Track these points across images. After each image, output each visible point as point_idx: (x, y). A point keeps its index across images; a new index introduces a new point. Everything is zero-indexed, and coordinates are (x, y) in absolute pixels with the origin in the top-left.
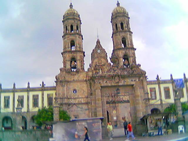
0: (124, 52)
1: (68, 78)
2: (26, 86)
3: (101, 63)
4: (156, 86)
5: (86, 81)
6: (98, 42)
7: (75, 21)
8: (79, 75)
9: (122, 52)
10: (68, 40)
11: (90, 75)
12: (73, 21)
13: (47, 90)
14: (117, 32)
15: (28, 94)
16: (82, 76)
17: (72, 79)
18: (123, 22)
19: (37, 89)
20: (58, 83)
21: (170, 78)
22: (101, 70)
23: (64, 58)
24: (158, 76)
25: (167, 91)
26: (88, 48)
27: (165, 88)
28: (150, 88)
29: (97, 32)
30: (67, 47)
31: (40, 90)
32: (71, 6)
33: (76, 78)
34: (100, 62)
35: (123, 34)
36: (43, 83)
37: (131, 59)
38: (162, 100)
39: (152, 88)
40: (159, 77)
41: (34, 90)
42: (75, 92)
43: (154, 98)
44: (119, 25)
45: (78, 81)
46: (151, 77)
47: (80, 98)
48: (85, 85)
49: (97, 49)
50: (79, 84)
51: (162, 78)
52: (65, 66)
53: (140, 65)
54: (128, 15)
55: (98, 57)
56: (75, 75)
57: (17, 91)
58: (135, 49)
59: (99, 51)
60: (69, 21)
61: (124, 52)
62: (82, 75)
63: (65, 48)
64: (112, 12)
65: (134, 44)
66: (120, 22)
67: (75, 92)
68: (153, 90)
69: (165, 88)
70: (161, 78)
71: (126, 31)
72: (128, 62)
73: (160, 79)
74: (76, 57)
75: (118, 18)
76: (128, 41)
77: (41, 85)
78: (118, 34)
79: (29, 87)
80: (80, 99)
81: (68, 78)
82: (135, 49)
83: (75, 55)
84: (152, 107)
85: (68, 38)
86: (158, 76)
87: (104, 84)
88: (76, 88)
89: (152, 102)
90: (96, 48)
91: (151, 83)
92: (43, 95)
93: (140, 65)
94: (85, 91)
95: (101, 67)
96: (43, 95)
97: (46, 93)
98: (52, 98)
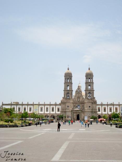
0: (89, 91)
4: (101, 107)
5: (73, 103)
13: (57, 105)
26: (75, 88)
29: (79, 82)
35: (89, 84)
46: (98, 102)
52: (65, 96)
54: (93, 75)
58: (94, 90)
60: (67, 77)
64: (86, 73)
66: (89, 76)
69: (104, 107)
82: (94, 90)
89: (99, 113)
91: (99, 105)
93: (95, 98)
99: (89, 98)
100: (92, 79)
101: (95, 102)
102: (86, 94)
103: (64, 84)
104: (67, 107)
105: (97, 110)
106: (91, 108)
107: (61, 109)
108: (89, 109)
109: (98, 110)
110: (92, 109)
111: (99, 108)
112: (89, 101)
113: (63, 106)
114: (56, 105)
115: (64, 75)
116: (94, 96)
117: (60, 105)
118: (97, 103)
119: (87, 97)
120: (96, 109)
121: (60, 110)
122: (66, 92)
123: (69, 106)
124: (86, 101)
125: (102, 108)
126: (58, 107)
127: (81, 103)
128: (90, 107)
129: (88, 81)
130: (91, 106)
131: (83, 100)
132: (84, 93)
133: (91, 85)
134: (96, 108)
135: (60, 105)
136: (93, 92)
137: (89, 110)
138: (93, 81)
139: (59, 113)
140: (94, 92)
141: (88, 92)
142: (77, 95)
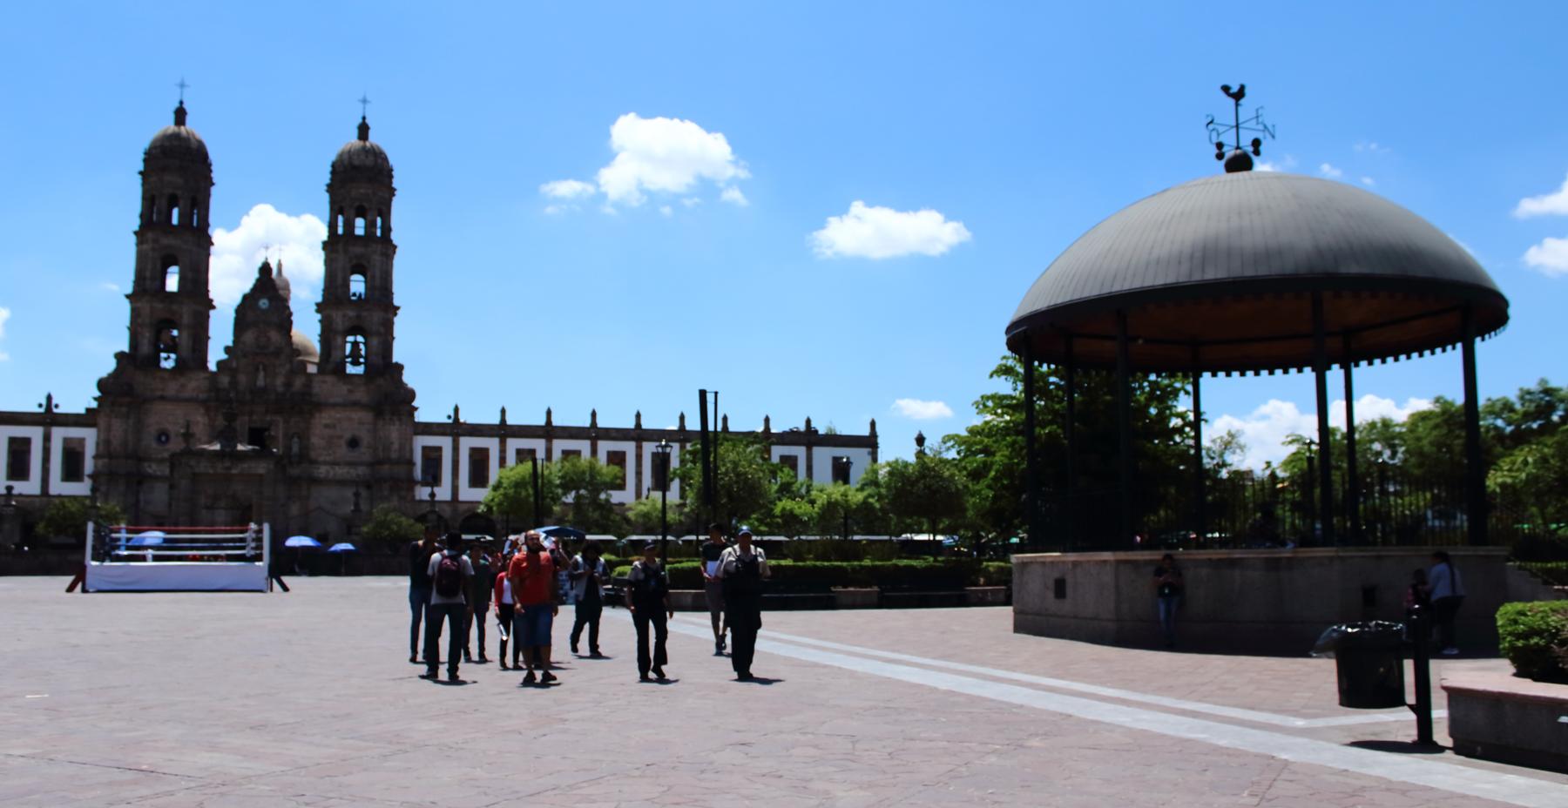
0: (351, 313)
8: (182, 380)
10: (154, 249)
16: (194, 384)
17: (159, 393)
26: (228, 283)
28: (424, 448)
30: (148, 274)
33: (172, 388)
35: (358, 250)
36: (49, 398)
43: (430, 479)
45: (176, 400)
46: (429, 410)
48: (199, 418)
53: (400, 367)
54: (391, 177)
59: (264, 303)
61: (351, 313)
62: (192, 384)
65: (395, 289)
68: (432, 456)
83: (175, 307)
85: (155, 241)
90: (255, 289)
92: (47, 438)
93: (400, 367)
96: (47, 438)
97: (59, 434)
99: (351, 369)
100: (385, 213)
101: (404, 399)
102: (327, 336)
103: (133, 239)
104: (154, 445)
105: (418, 473)
106: (364, 453)
107: (96, 457)
108: (351, 464)
109: (424, 471)
110: (375, 463)
111: (434, 455)
112: (350, 391)
113: (118, 427)
114: (49, 418)
115: (141, 167)
116: (396, 358)
117: (86, 419)
118: (422, 416)
119: (336, 356)
120: (411, 463)
121: (89, 465)
122: (145, 306)
123: (171, 428)
124: (328, 388)
125: (456, 456)
126: (66, 441)
128: (354, 443)
129: (349, 226)
130: (365, 437)
131: (299, 382)
132: (306, 329)
133: (377, 258)
134: (411, 451)
136: (388, 327)
137: (341, 471)
138: (387, 229)
139: (82, 488)
142: (249, 337)
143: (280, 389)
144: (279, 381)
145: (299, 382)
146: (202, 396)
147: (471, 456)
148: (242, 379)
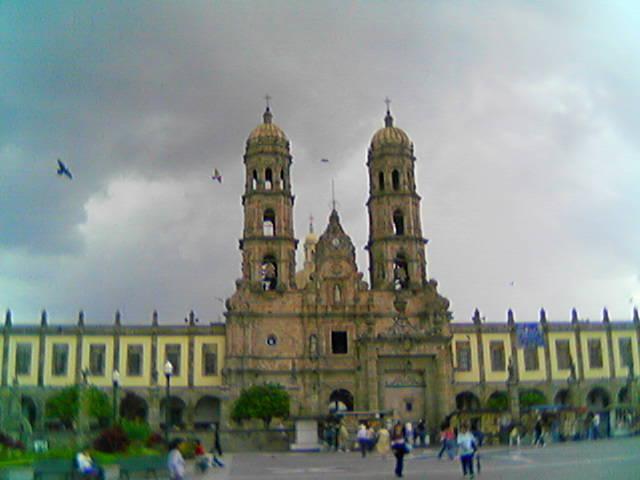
0: (397, 247)
1: (257, 305)
2: (150, 322)
3: (340, 273)
5: (301, 316)
6: (334, 218)
7: (277, 160)
9: (392, 248)
11: (310, 302)
12: (273, 160)
14: (382, 196)
15: (154, 341)
16: (291, 303)
17: (267, 309)
18: (399, 171)
19: (177, 330)
20: (233, 319)
21: (506, 319)
22: (340, 289)
23: (247, 255)
24: (477, 313)
25: (498, 351)
27: (493, 344)
29: (332, 192)
31: (182, 334)
32: (267, 116)
33: (276, 306)
34: (338, 269)
35: (396, 202)
36: (192, 315)
37: (414, 268)
38: (481, 374)
39: (462, 343)
40: (481, 316)
41: (169, 331)
42: (271, 342)
43: (465, 366)
44: (389, 178)
46: (461, 314)
47: (284, 358)
49: (331, 236)
50: (282, 323)
51: (489, 317)
52: (248, 275)
54: (412, 151)
55: (332, 257)
56: (275, 299)
57: (124, 334)
58: (426, 242)
59: (335, 242)
60: (263, 158)
61: (397, 247)
62: (291, 302)
63: (248, 228)
66: (391, 169)
67: (271, 342)
68: (463, 348)
70: (484, 319)
71: (403, 195)
72: (407, 273)
73: (482, 321)
74: (278, 253)
75: (387, 158)
76: (409, 222)
77: (186, 320)
78: (385, 199)
79: (155, 324)
80: (285, 362)
81: (257, 305)
82: (426, 242)
83: (275, 247)
84: (459, 390)
85: (259, 201)
86: (477, 313)
87: (387, 349)
88: (275, 333)
90: (328, 231)
91: (461, 328)
92: (191, 345)
93: (434, 284)
94: (297, 342)
95: (340, 282)
96: (191, 345)
98: (213, 355)
114: (192, 330)
117: (218, 329)
118: (457, 319)
121: (220, 365)
123: (278, 335)
127: (353, 316)
135: (224, 334)
140: (426, 247)
141: (390, 251)
143: (352, 303)
144: (350, 297)
145: (364, 298)
146: (298, 311)
147: (491, 348)
148: (323, 296)
